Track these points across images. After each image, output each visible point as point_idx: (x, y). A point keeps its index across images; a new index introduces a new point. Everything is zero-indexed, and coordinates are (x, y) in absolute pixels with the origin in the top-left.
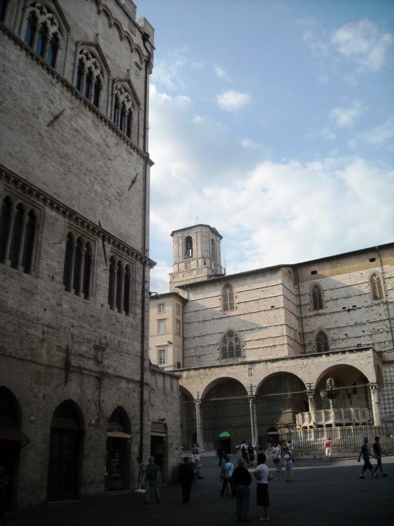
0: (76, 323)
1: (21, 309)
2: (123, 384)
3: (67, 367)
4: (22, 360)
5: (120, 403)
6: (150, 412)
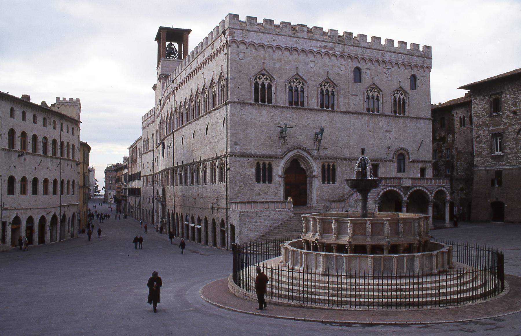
3: (212, 208)
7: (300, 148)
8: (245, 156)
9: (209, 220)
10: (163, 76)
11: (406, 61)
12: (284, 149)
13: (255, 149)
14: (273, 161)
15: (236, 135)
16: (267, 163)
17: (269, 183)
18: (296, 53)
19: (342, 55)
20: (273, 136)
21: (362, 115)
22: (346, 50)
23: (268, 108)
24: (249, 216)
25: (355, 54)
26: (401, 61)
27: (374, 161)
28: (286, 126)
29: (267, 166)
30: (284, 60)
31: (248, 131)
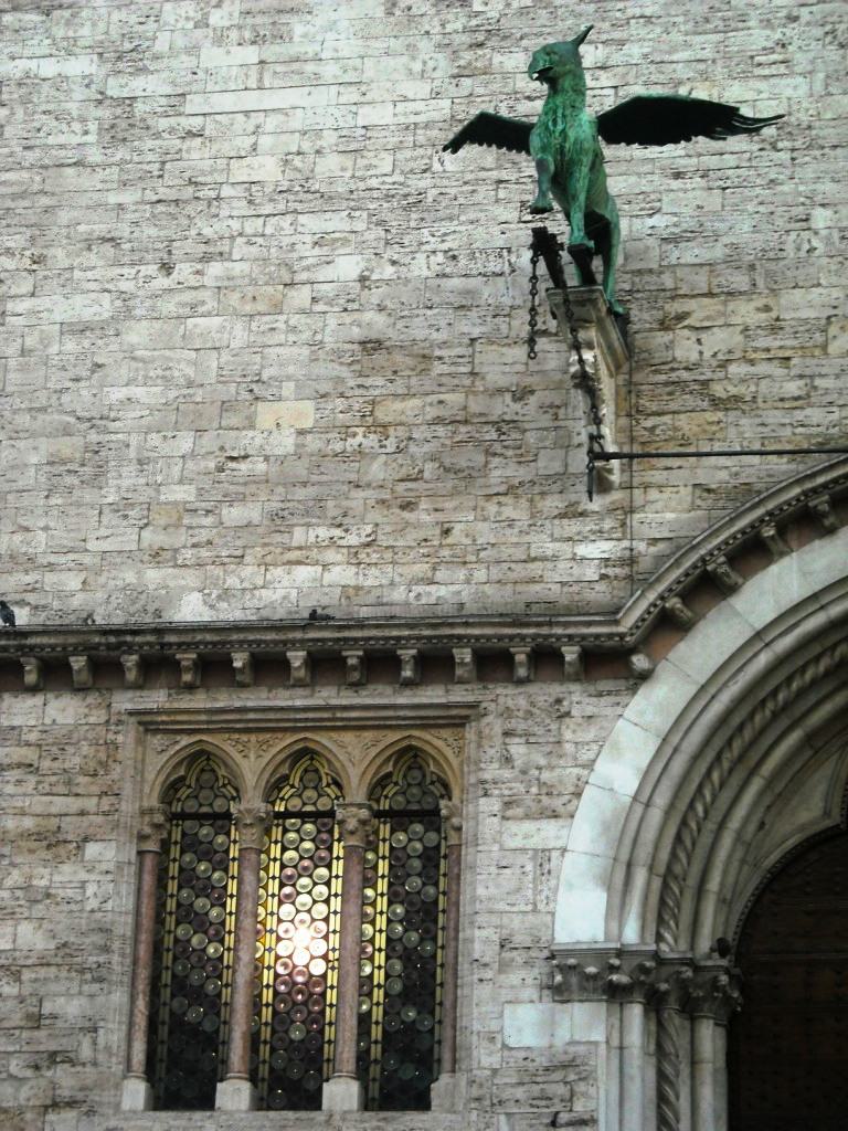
13: (157, 556)
14: (457, 720)
17: (367, 1104)
20: (470, 326)
31: (62, 308)
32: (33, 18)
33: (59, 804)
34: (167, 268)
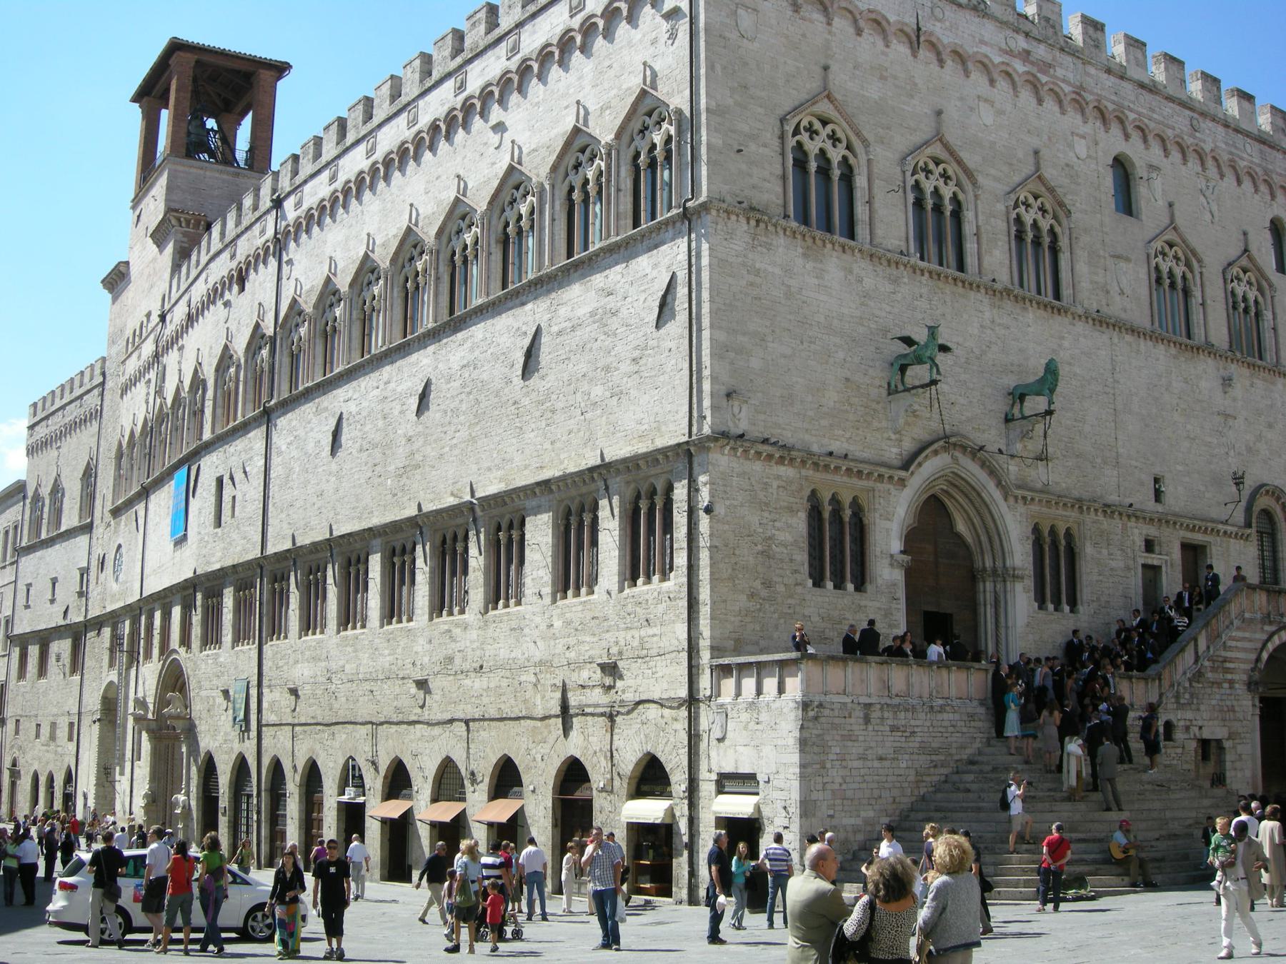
0: (572, 641)
1: (513, 655)
2: (652, 712)
3: (565, 713)
4: (518, 719)
5: (649, 748)
6: (713, 754)
7: (964, 448)
8: (770, 457)
9: (528, 768)
10: (179, 220)
11: (1260, 165)
12: (908, 446)
15: (732, 355)
16: (846, 499)
18: (931, 56)
19: (1078, 97)
21: (1150, 343)
22: (1089, 82)
23: (847, 257)
24: (835, 727)
25: (1113, 102)
26: (1242, 158)
27: (1193, 530)
28: (933, 331)
29: (847, 514)
30: (895, 78)
32: (764, 250)
33: (792, 500)
34: (802, 343)
